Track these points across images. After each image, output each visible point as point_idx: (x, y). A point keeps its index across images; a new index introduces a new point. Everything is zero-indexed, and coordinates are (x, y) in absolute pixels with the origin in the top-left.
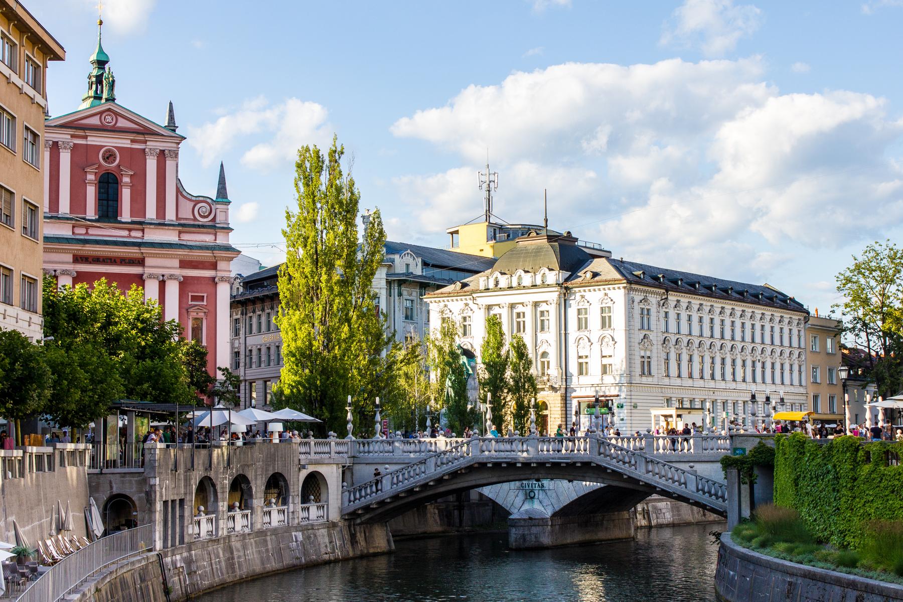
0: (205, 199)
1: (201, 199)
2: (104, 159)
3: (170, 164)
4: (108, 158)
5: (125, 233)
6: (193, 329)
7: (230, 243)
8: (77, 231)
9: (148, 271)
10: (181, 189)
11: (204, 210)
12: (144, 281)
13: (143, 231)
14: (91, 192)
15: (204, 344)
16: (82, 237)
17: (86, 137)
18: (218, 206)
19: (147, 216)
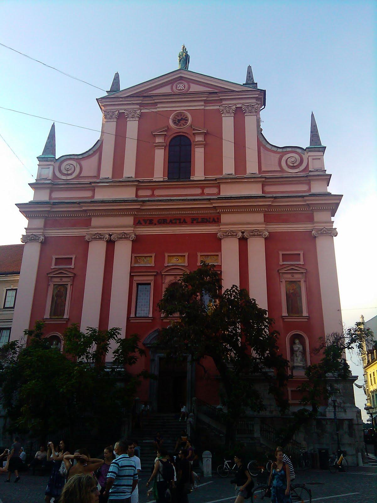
0: (293, 149)
1: (288, 149)
2: (175, 123)
3: (250, 121)
4: (179, 121)
5: (199, 191)
6: (288, 296)
7: (328, 191)
8: (141, 193)
9: (223, 228)
10: (264, 142)
11: (293, 159)
12: (220, 240)
13: (219, 187)
14: (160, 156)
15: (305, 314)
16: (147, 199)
17: (156, 104)
18: (310, 154)
19: (225, 172)
